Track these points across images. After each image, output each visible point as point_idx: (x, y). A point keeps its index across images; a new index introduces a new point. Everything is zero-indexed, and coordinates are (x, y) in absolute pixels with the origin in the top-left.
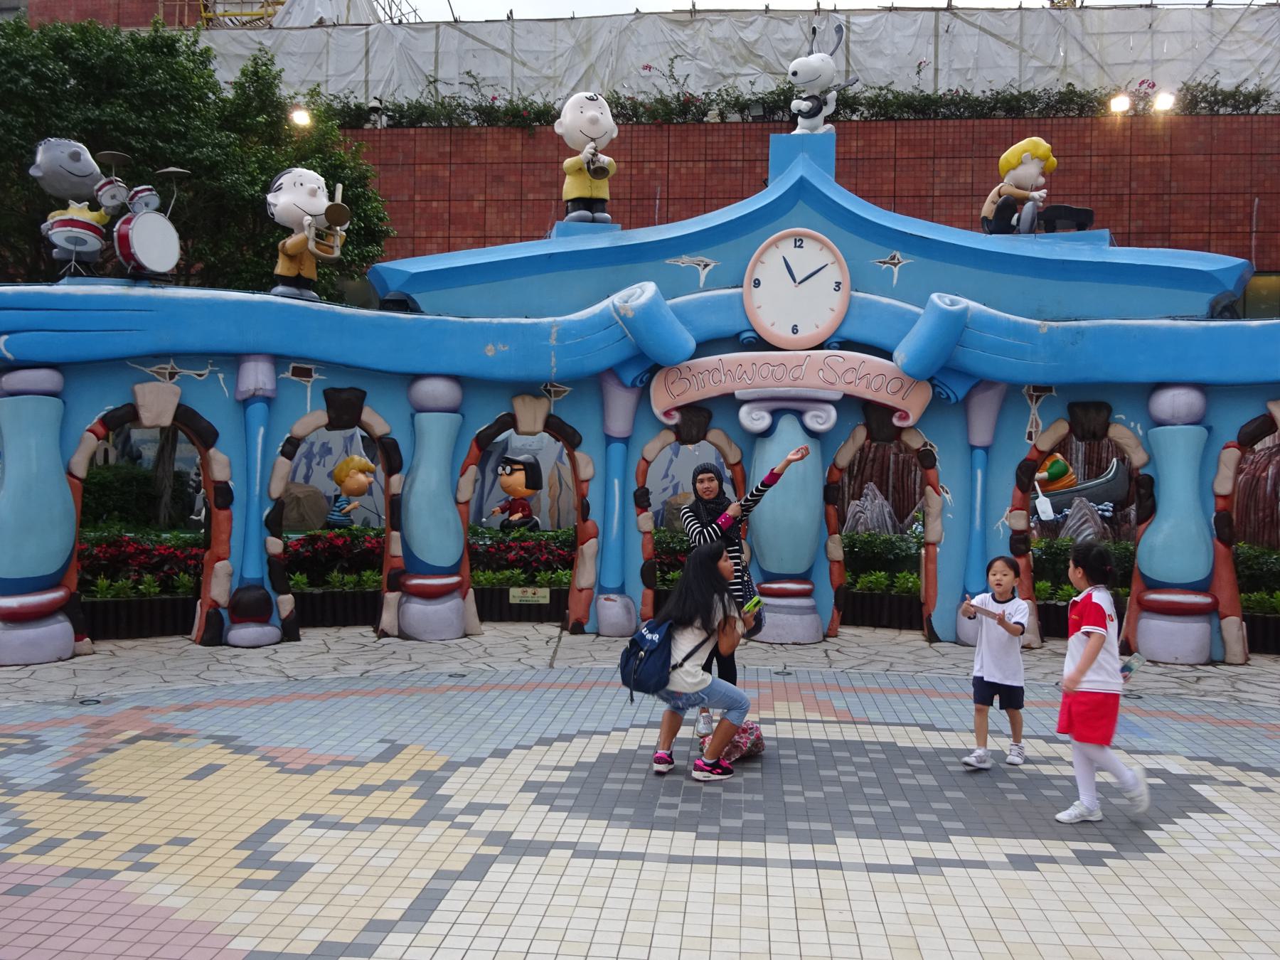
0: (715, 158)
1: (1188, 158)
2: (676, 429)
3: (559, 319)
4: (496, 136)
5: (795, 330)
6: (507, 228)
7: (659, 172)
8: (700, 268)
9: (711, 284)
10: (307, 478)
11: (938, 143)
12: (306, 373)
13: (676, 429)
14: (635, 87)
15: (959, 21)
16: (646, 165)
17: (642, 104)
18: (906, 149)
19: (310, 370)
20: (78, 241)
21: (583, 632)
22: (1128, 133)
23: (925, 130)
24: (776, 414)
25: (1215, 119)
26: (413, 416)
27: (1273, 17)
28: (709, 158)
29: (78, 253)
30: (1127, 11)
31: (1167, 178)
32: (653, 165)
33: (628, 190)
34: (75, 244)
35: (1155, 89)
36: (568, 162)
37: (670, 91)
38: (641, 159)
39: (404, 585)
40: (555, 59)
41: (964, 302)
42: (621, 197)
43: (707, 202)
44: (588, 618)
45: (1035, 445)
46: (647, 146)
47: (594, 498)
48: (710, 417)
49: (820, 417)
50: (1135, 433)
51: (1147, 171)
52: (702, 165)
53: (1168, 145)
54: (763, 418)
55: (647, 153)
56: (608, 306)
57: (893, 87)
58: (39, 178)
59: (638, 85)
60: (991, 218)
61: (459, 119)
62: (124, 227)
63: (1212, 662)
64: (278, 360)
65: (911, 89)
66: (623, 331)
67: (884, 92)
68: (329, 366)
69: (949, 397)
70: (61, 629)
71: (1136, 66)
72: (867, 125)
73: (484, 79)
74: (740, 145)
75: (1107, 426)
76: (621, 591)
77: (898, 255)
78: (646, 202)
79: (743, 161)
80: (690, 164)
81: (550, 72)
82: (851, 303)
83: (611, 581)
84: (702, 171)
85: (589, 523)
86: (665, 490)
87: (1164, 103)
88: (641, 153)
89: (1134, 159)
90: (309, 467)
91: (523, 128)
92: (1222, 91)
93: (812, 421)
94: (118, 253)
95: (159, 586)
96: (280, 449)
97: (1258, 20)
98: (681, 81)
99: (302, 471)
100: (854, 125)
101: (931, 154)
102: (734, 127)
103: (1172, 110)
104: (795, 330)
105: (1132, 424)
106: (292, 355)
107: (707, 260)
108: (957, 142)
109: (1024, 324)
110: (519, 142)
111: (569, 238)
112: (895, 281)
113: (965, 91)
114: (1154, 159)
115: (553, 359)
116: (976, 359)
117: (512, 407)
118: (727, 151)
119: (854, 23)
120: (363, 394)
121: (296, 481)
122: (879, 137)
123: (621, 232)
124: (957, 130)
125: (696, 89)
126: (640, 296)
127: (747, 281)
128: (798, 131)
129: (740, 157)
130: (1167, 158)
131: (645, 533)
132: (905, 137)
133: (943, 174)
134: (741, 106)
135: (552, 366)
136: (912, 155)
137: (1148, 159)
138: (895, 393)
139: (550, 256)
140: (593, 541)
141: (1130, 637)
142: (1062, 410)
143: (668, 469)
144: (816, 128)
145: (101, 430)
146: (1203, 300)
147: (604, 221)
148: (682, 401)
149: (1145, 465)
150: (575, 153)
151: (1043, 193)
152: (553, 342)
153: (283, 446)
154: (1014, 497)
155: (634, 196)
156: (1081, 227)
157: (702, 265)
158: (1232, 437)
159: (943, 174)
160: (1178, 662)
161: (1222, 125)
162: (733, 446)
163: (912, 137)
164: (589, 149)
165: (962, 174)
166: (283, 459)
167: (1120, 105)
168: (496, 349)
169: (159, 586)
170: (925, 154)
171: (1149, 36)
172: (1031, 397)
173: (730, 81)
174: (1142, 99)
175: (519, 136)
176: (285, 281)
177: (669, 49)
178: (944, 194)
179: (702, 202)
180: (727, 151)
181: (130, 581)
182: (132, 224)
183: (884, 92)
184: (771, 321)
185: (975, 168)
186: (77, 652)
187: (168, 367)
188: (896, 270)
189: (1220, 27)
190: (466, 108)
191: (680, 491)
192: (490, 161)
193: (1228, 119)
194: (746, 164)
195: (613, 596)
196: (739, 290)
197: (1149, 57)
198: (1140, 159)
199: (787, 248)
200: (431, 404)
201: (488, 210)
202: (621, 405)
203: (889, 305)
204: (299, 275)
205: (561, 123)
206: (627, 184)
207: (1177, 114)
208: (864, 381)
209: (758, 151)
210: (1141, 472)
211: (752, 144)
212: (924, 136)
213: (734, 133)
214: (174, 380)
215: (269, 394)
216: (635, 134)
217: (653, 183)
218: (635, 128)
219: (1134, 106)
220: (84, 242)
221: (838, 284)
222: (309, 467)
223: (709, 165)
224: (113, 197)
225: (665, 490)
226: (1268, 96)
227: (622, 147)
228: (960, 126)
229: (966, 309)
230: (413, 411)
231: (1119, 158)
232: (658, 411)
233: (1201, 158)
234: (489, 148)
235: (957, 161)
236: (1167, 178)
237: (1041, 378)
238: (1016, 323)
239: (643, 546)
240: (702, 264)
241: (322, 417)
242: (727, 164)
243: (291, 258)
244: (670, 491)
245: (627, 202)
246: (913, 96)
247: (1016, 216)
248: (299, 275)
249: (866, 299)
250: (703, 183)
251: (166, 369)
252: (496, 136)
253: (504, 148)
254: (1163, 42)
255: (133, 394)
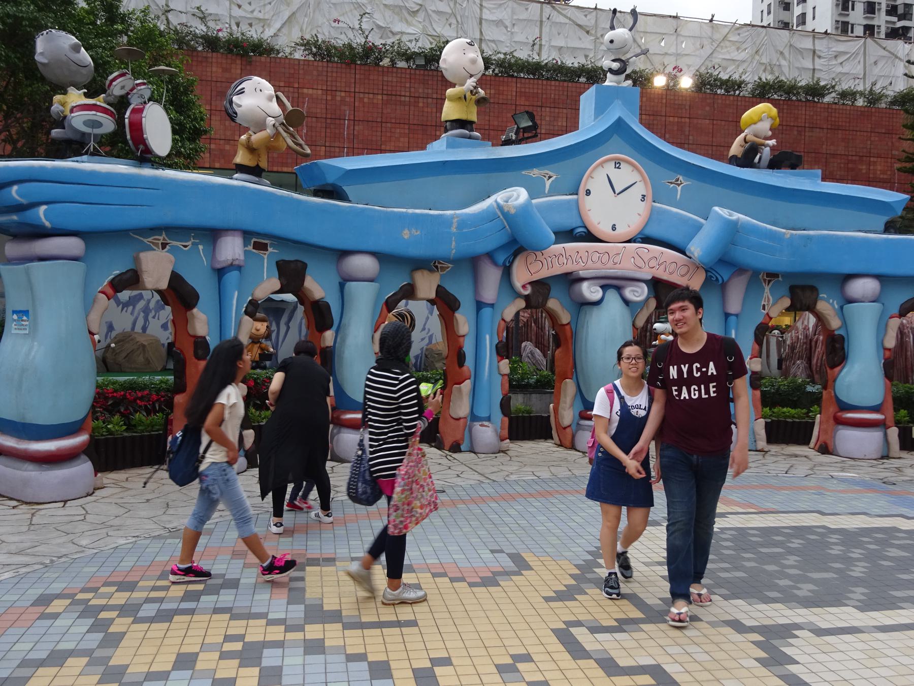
0: (389, 93)
1: (700, 121)
2: (527, 298)
3: (458, 212)
4: (219, 60)
5: (614, 228)
6: (228, 133)
7: (348, 99)
8: (546, 179)
9: (554, 191)
10: (144, 329)
11: (544, 96)
12: (263, 247)
13: (527, 298)
14: (327, 34)
15: (556, 12)
16: (338, 93)
17: (335, 48)
18: (523, 99)
19: (267, 244)
20: (97, 124)
21: (460, 451)
22: (664, 101)
23: (536, 86)
24: (604, 288)
25: (716, 97)
26: (342, 286)
27: (747, 33)
28: (385, 92)
29: (95, 135)
30: (663, 19)
31: (687, 133)
32: (343, 94)
33: (324, 111)
34: (93, 127)
35: (682, 73)
36: (450, 91)
37: (358, 40)
38: (334, 89)
39: (338, 418)
40: (265, 5)
41: (736, 216)
42: (319, 116)
43: (384, 125)
44: (463, 439)
45: (768, 314)
46: (339, 79)
47: (468, 348)
48: (549, 290)
49: (637, 292)
50: (832, 305)
51: (675, 128)
52: (380, 97)
53: (688, 111)
54: (598, 291)
55: (338, 84)
56: (491, 204)
57: (515, 54)
58: (43, 64)
59: (329, 32)
60: (740, 156)
61: (188, 44)
62: (136, 116)
63: (883, 458)
64: (247, 235)
65: (526, 57)
66: (503, 224)
67: (508, 57)
68: (281, 241)
69: (717, 279)
70: (85, 467)
71: (667, 56)
72: (497, 79)
73: (211, 14)
74: (408, 85)
75: (815, 303)
76: (489, 419)
77: (681, 178)
78: (337, 122)
79: (410, 96)
80: (371, 96)
81: (260, 16)
82: (653, 211)
83: (482, 412)
84: (380, 102)
85: (464, 368)
86: (423, 339)
87: (686, 83)
88: (334, 84)
89: (668, 119)
90: (146, 319)
91: (242, 56)
92: (720, 79)
93: (629, 293)
94: (128, 137)
95: (125, 424)
96: (244, 309)
97: (739, 34)
98: (367, 33)
99: (140, 323)
100: (488, 78)
101: (540, 104)
102: (399, 71)
103: (690, 88)
104: (614, 228)
105: (831, 301)
106: (262, 231)
107: (551, 173)
108: (557, 97)
109: (775, 231)
110: (239, 67)
111: (456, 150)
112: (678, 197)
113: (562, 62)
114: (680, 120)
115: (454, 243)
116: (746, 255)
117: (412, 278)
118: (398, 88)
119: (485, 7)
120: (305, 266)
121: (136, 331)
122: (505, 88)
123: (491, 148)
124: (557, 88)
125: (376, 40)
126: (517, 199)
127: (582, 191)
128: (607, 83)
129: (408, 94)
130: (687, 120)
131: (503, 375)
132: (523, 90)
133: (548, 119)
134: (408, 56)
135: (453, 248)
136: (527, 103)
137: (676, 119)
138: (683, 276)
139: (444, 163)
140: (468, 382)
141: (828, 442)
142: (785, 290)
143: (425, 325)
144: (619, 83)
145: (110, 291)
146: (882, 220)
147: (476, 138)
148: (536, 277)
149: (839, 328)
150: (453, 85)
151: (772, 142)
152: (454, 230)
153: (246, 307)
154: (753, 349)
155: (329, 116)
156: (793, 167)
157: (548, 176)
158: (896, 311)
159: (548, 119)
160: (866, 458)
161: (720, 101)
162: (565, 311)
163: (527, 90)
164: (471, 83)
165: (560, 119)
166: (247, 318)
167: (659, 81)
168: (410, 233)
169: (125, 424)
170: (535, 104)
171: (675, 37)
172: (765, 280)
173: (398, 37)
174: (673, 79)
175: (238, 62)
176: (241, 168)
177: (352, 8)
178: (548, 132)
179: (379, 125)
180: (398, 88)
181: (100, 421)
182: (145, 113)
183: (508, 57)
184: (599, 222)
185: (569, 116)
186: (97, 487)
187: (161, 238)
188: (679, 188)
189: (718, 36)
190: (195, 36)
191: (434, 341)
192: (214, 79)
193: (724, 97)
194: (412, 100)
195: (486, 423)
196: (575, 197)
197: (675, 51)
198: (671, 119)
199: (610, 168)
200: (360, 275)
201: (213, 118)
202: (491, 277)
203: (677, 214)
204: (258, 165)
205: (445, 60)
206: (323, 106)
207: (693, 91)
208: (662, 267)
209: (421, 91)
210: (836, 333)
211: (416, 85)
212: (535, 91)
213: (403, 76)
214: (166, 250)
215: (242, 263)
216: (329, 69)
217: (343, 108)
218: (330, 65)
219: (668, 85)
220: (98, 124)
221: (644, 196)
222: (146, 319)
223: (385, 97)
224: (123, 87)
225: (423, 339)
226: (746, 84)
227: (320, 78)
228: (547, 85)
229: (738, 219)
230: (341, 281)
231: (659, 118)
232: (518, 284)
233: (707, 121)
234: (214, 69)
235: (557, 110)
236: (687, 133)
237: (773, 268)
238: (771, 230)
239: (502, 385)
240: (547, 176)
241: (276, 284)
242: (398, 98)
243: (251, 149)
244: (426, 341)
245: (324, 120)
246: (528, 62)
247: (758, 157)
248: (258, 165)
249: (661, 208)
250: (380, 111)
251: (159, 240)
252: (219, 60)
253: (225, 70)
254: (682, 42)
255: (137, 260)
